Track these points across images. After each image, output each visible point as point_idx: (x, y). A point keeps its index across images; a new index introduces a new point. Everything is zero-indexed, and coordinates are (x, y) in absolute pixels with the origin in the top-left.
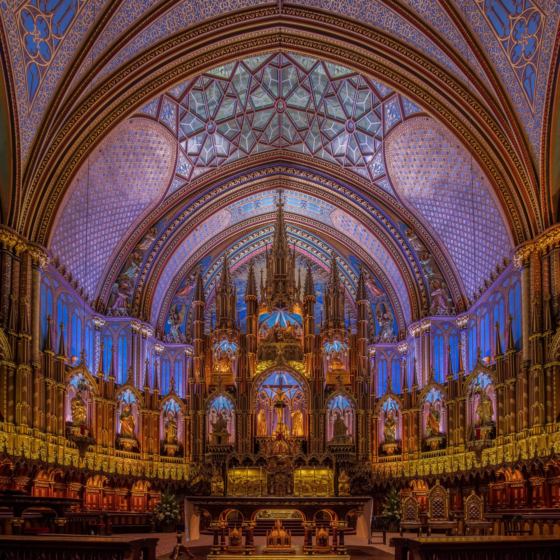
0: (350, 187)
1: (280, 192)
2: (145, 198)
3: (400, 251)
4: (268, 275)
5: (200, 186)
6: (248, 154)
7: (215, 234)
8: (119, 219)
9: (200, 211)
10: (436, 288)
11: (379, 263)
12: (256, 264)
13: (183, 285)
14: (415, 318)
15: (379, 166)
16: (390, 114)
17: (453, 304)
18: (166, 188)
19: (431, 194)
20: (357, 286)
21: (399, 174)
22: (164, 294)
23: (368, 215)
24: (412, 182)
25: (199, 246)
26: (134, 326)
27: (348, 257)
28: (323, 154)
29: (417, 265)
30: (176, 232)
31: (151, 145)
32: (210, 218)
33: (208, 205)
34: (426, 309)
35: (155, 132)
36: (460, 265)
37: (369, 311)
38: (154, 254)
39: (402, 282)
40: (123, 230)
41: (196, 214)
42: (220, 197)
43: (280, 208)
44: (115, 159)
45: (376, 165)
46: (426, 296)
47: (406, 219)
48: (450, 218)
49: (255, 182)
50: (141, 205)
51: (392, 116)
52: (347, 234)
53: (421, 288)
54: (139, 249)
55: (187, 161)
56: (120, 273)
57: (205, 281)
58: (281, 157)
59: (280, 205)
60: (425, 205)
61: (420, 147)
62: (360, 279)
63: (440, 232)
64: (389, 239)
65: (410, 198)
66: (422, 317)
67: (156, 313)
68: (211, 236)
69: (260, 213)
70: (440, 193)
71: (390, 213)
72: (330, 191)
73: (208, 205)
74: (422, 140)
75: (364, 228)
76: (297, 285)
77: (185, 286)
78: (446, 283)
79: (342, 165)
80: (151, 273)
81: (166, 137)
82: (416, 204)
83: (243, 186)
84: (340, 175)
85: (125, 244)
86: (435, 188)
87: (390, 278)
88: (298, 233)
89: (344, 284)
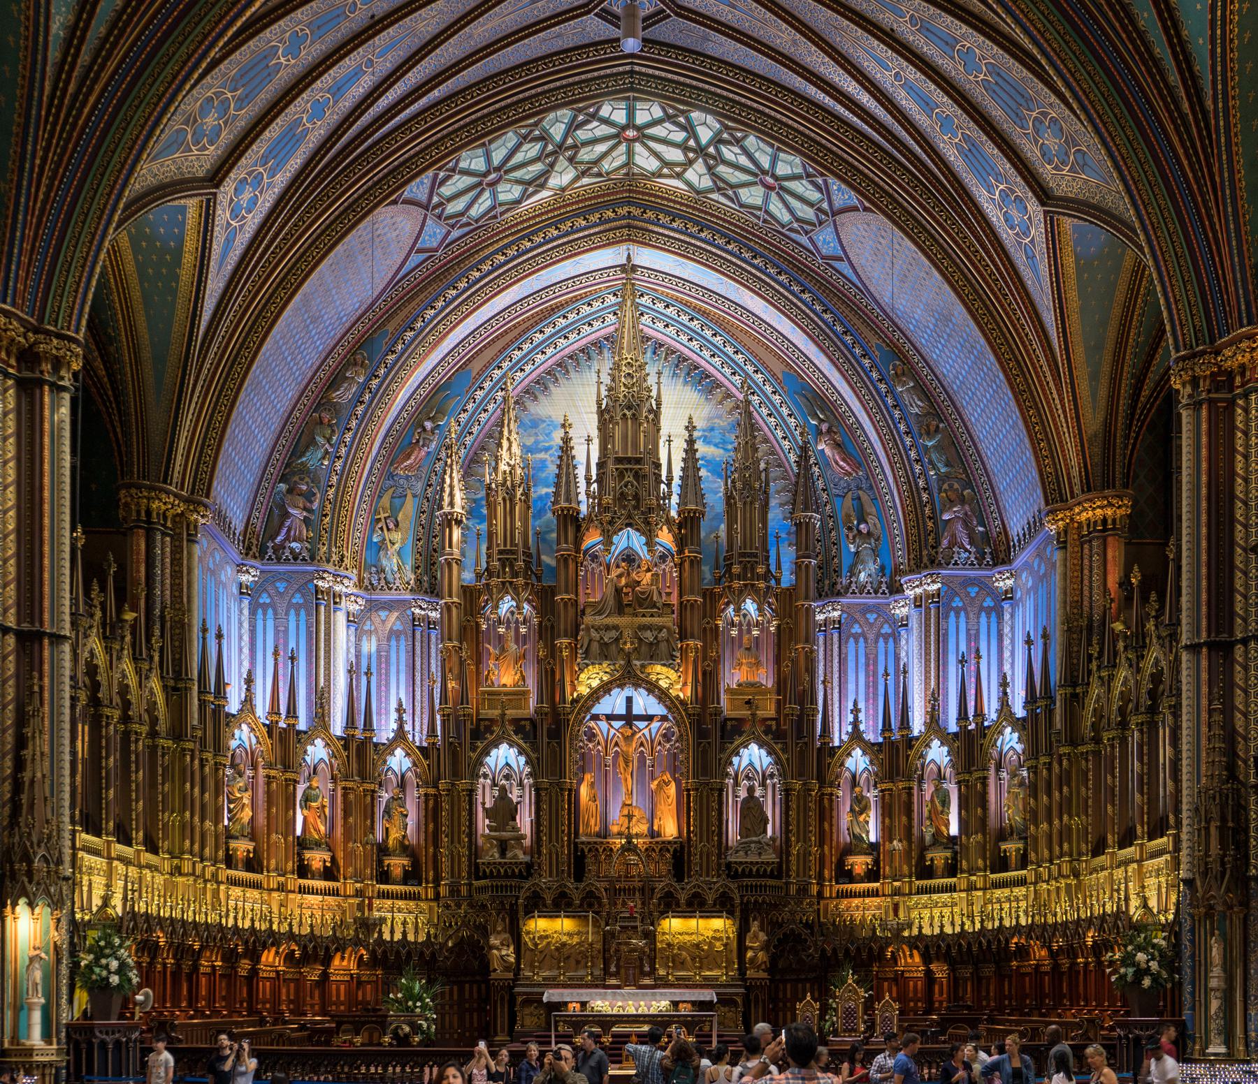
0: (776, 259)
17: (986, 537)
26: (320, 583)
34: (933, 547)
38: (360, 410)
47: (891, 341)
53: (925, 496)
58: (630, 191)
66: (926, 567)
71: (858, 323)
78: (973, 490)
84: (754, 235)
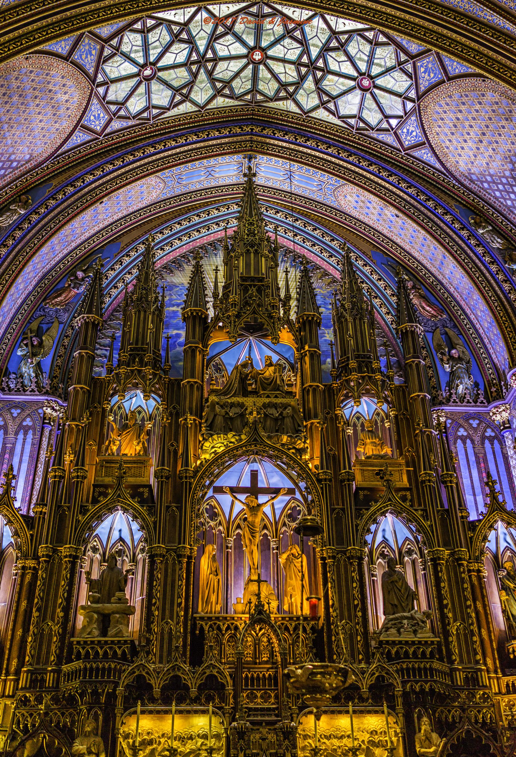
0: (367, 156)
1: (250, 158)
9: (112, 176)
15: (412, 132)
18: (59, 142)
21: (448, 142)
22: (20, 301)
28: (322, 114)
30: (66, 204)
32: (128, 187)
33: (127, 168)
41: (104, 180)
42: (150, 159)
43: (250, 180)
45: (408, 130)
47: (467, 202)
49: (210, 143)
50: (12, 162)
58: (253, 114)
59: (250, 175)
64: (442, 229)
71: (438, 193)
72: (333, 160)
73: (127, 168)
75: (397, 212)
79: (353, 128)
82: (482, 182)
83: (190, 147)
84: (349, 140)
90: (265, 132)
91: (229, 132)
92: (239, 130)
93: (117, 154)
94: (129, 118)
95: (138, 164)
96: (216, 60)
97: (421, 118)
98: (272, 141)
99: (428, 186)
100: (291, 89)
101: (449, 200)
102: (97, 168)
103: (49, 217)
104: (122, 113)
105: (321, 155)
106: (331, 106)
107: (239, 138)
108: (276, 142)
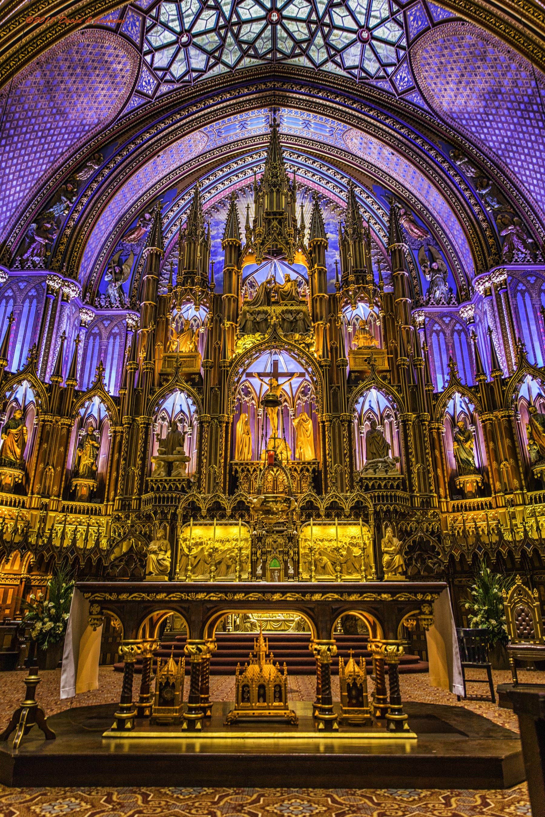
0: (368, 103)
2: (91, 117)
3: (446, 178)
4: (257, 212)
5: (167, 104)
6: (233, 68)
7: (183, 161)
8: (51, 142)
9: (164, 133)
10: (506, 226)
11: (417, 195)
12: (241, 199)
13: (133, 226)
14: (480, 267)
15: (405, 77)
16: (414, 20)
18: (120, 107)
19: (480, 107)
20: (388, 225)
21: (434, 86)
22: (103, 239)
23: (396, 134)
24: (452, 94)
25: (161, 176)
27: (371, 187)
28: (330, 67)
29: (473, 195)
30: (130, 159)
31: (106, 58)
32: (179, 141)
33: (176, 126)
35: (113, 44)
36: (537, 194)
37: (409, 259)
39: (453, 218)
40: (55, 156)
41: (158, 137)
42: (194, 117)
43: (275, 130)
44: (56, 73)
45: (401, 76)
46: (494, 236)
47: (449, 138)
48: (512, 134)
49: (241, 99)
50: (84, 126)
51: (417, 23)
52: (369, 159)
53: (484, 225)
54: (74, 180)
55: (151, 76)
56: (42, 210)
57: (165, 221)
58: (274, 71)
59: (275, 125)
60: (473, 120)
61: (457, 54)
62: (391, 215)
63: (500, 152)
64: (427, 163)
65: (451, 113)
66: (492, 266)
67: (88, 265)
68: (179, 164)
69: (247, 136)
70: (493, 105)
71: (425, 131)
72: (341, 108)
73: (176, 126)
74: (460, 46)
75: (392, 151)
76: (299, 226)
77: (136, 229)
78: (520, 218)
80: (88, 210)
81: (127, 50)
82: (461, 120)
83: (225, 104)
85: (55, 173)
86: (485, 99)
87: (435, 214)
88: (300, 159)
89: (368, 222)
90: (285, 87)
91: (256, 88)
92: (263, 87)
93: (167, 114)
94: (173, 82)
95: (184, 121)
96: (241, 23)
97: (411, 65)
98: (291, 95)
99: (417, 126)
100: (304, 46)
101: (434, 137)
102: (152, 127)
103: (118, 170)
104: (168, 77)
105: (331, 104)
106: (338, 59)
107: (264, 94)
108: (294, 95)
